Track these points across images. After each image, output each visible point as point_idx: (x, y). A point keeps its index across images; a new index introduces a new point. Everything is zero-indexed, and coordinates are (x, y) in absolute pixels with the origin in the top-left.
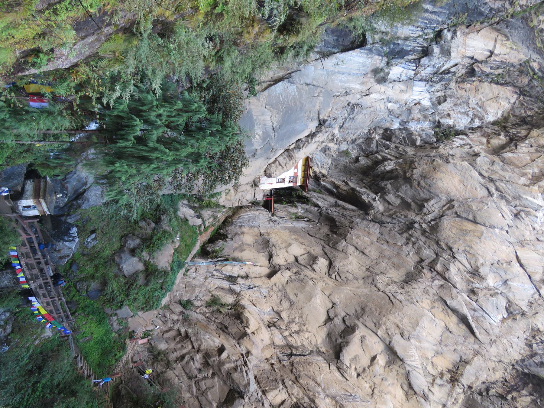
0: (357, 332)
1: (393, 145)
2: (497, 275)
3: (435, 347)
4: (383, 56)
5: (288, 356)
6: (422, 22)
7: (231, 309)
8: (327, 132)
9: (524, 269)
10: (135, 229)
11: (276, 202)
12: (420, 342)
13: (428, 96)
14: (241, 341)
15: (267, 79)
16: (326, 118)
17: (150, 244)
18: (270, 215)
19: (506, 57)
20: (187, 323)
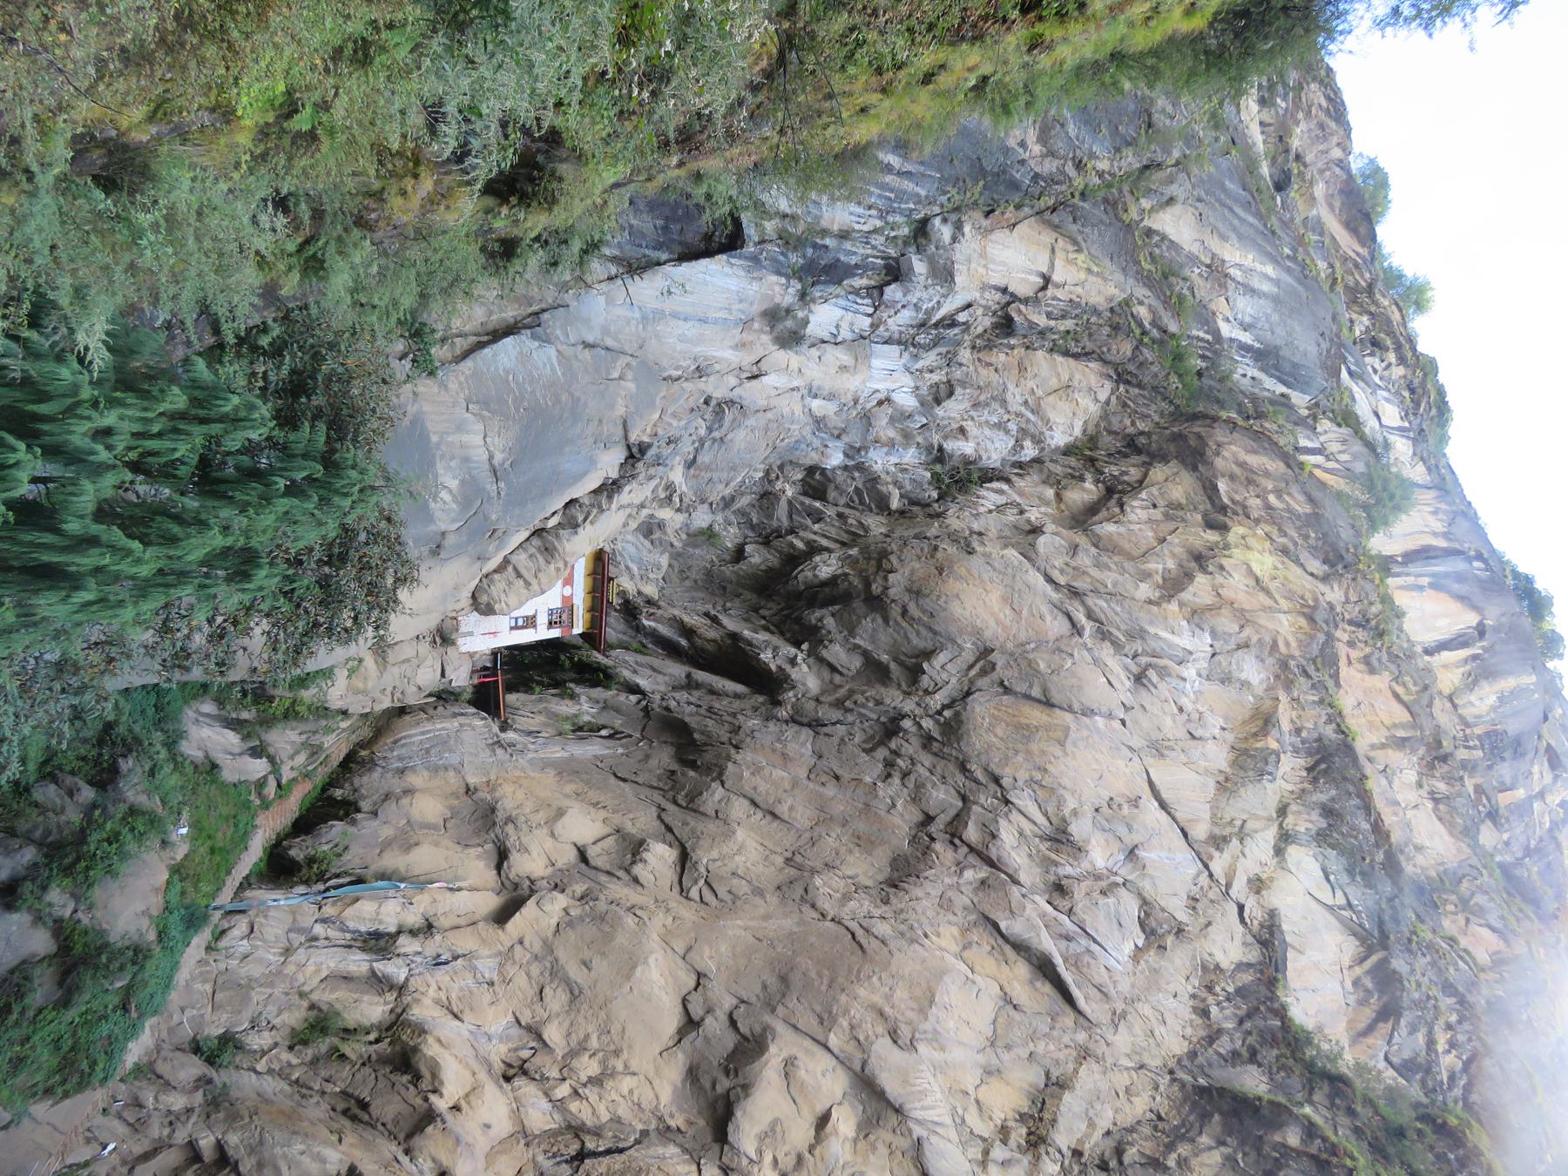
0: (773, 1049)
1: (830, 512)
2: (1110, 837)
3: (981, 1059)
4: (788, 277)
5: (573, 1158)
6: (880, 196)
7: (377, 1041)
8: (651, 478)
9: (1169, 814)
10: (17, 815)
11: (510, 688)
12: (943, 1049)
13: (908, 381)
14: (417, 1141)
15: (467, 328)
17: (78, 860)
18: (496, 729)
19: (1079, 290)
20: (221, 1115)
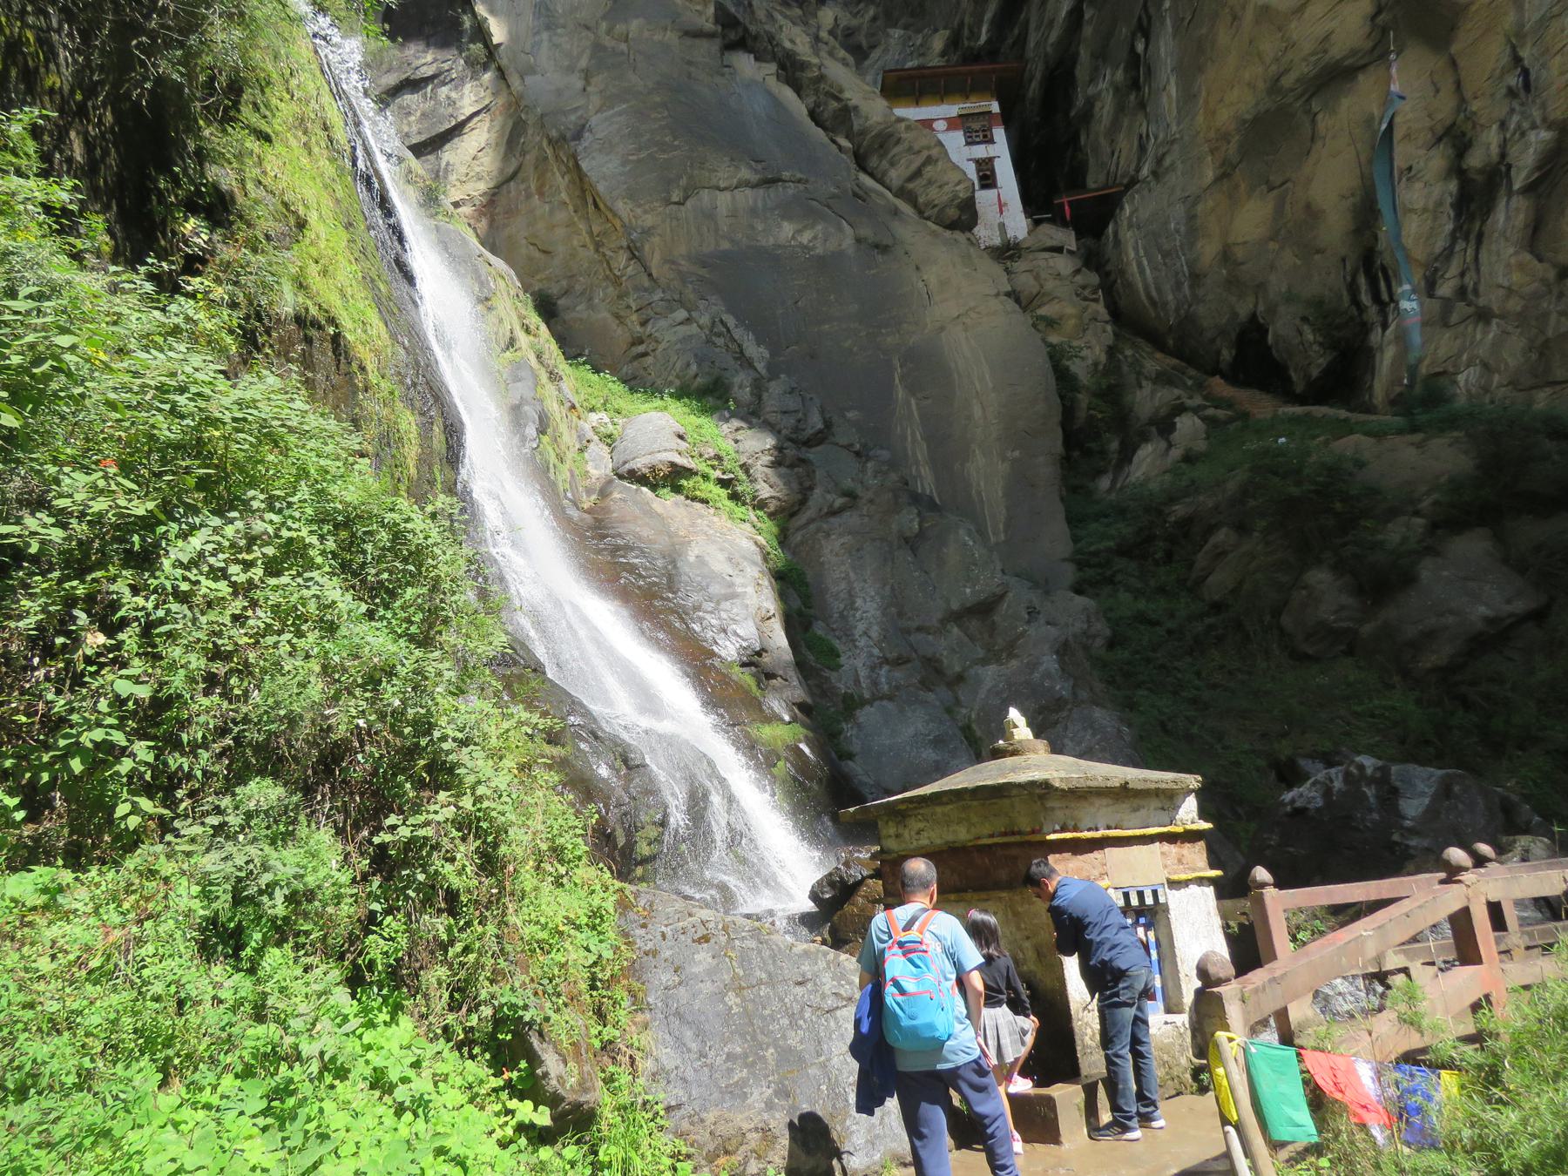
8: (771, 17)
16: (711, 10)
